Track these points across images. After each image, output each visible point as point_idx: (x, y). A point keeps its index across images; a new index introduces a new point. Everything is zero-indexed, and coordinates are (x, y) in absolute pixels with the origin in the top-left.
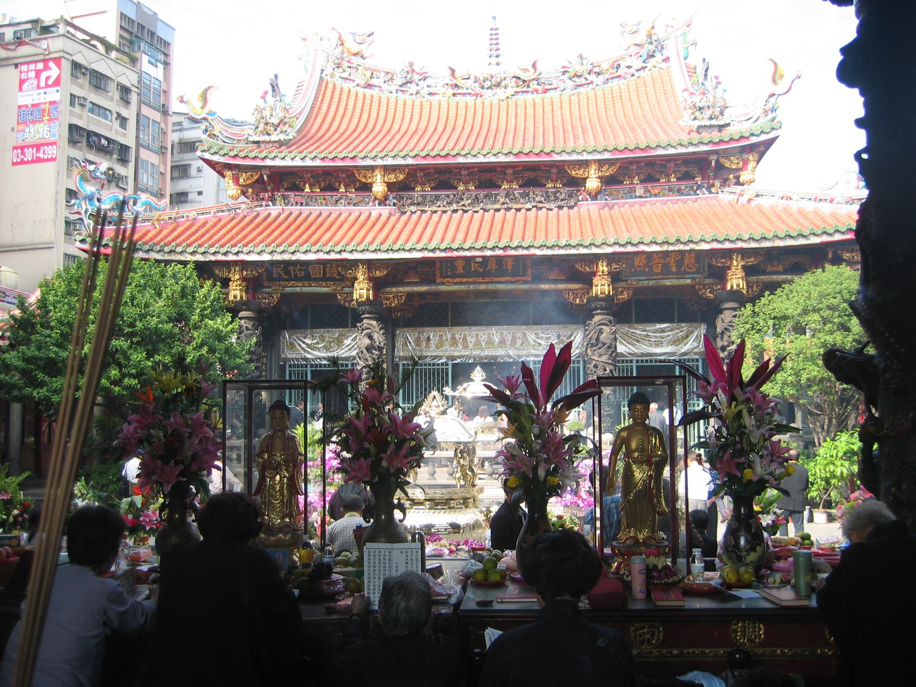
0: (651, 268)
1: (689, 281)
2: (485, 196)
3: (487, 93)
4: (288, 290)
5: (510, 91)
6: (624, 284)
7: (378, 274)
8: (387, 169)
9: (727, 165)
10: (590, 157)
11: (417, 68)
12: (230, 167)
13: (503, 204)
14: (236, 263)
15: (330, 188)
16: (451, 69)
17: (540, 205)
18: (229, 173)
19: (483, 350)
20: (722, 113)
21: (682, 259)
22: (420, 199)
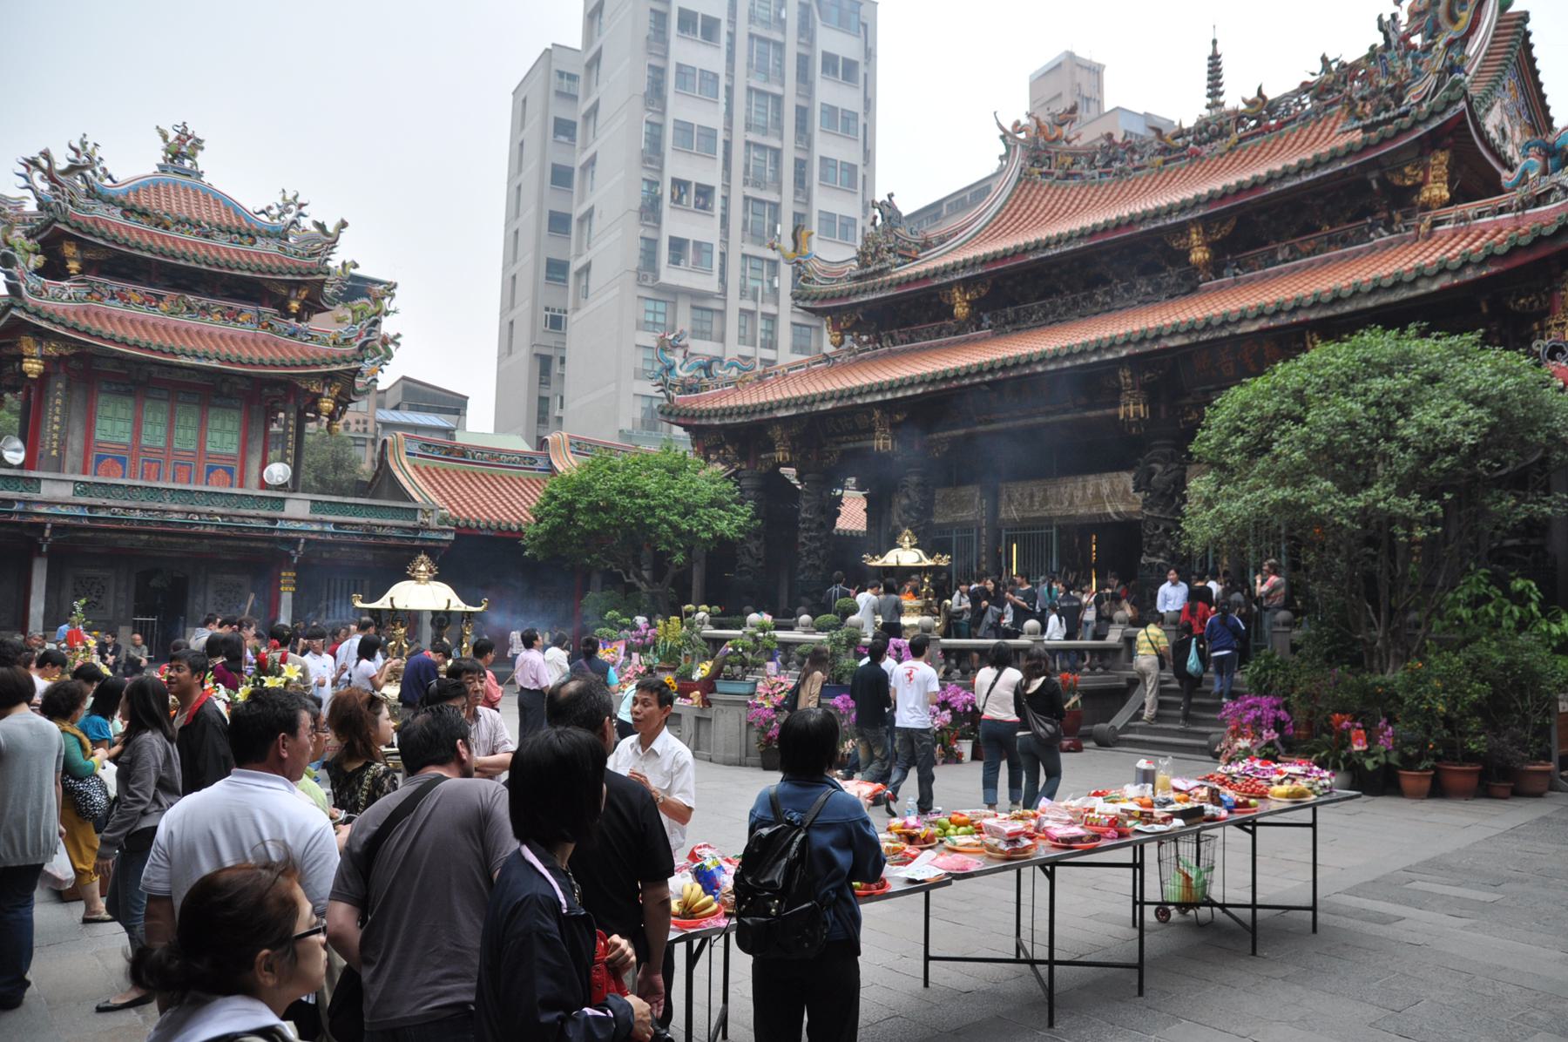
2: (1084, 298)
3: (1206, 149)
4: (844, 446)
5: (1234, 138)
6: (1189, 400)
9: (1397, 181)
10: (1182, 218)
11: (1118, 138)
13: (1104, 304)
14: (777, 420)
16: (1153, 129)
19: (1090, 506)
20: (1399, 101)
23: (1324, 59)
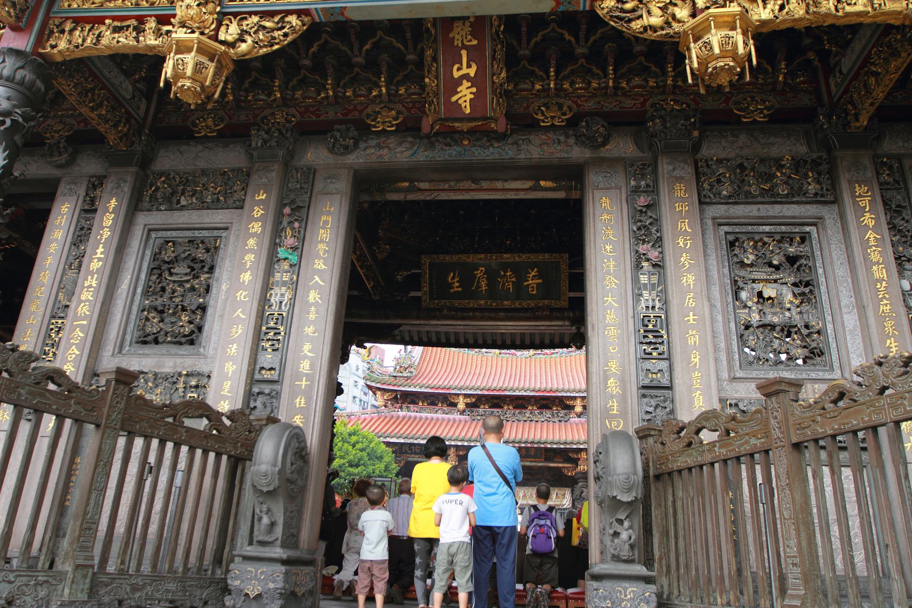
4: (410, 459)
7: (461, 453)
8: (466, 396)
12: (379, 389)
15: (433, 404)
18: (379, 393)
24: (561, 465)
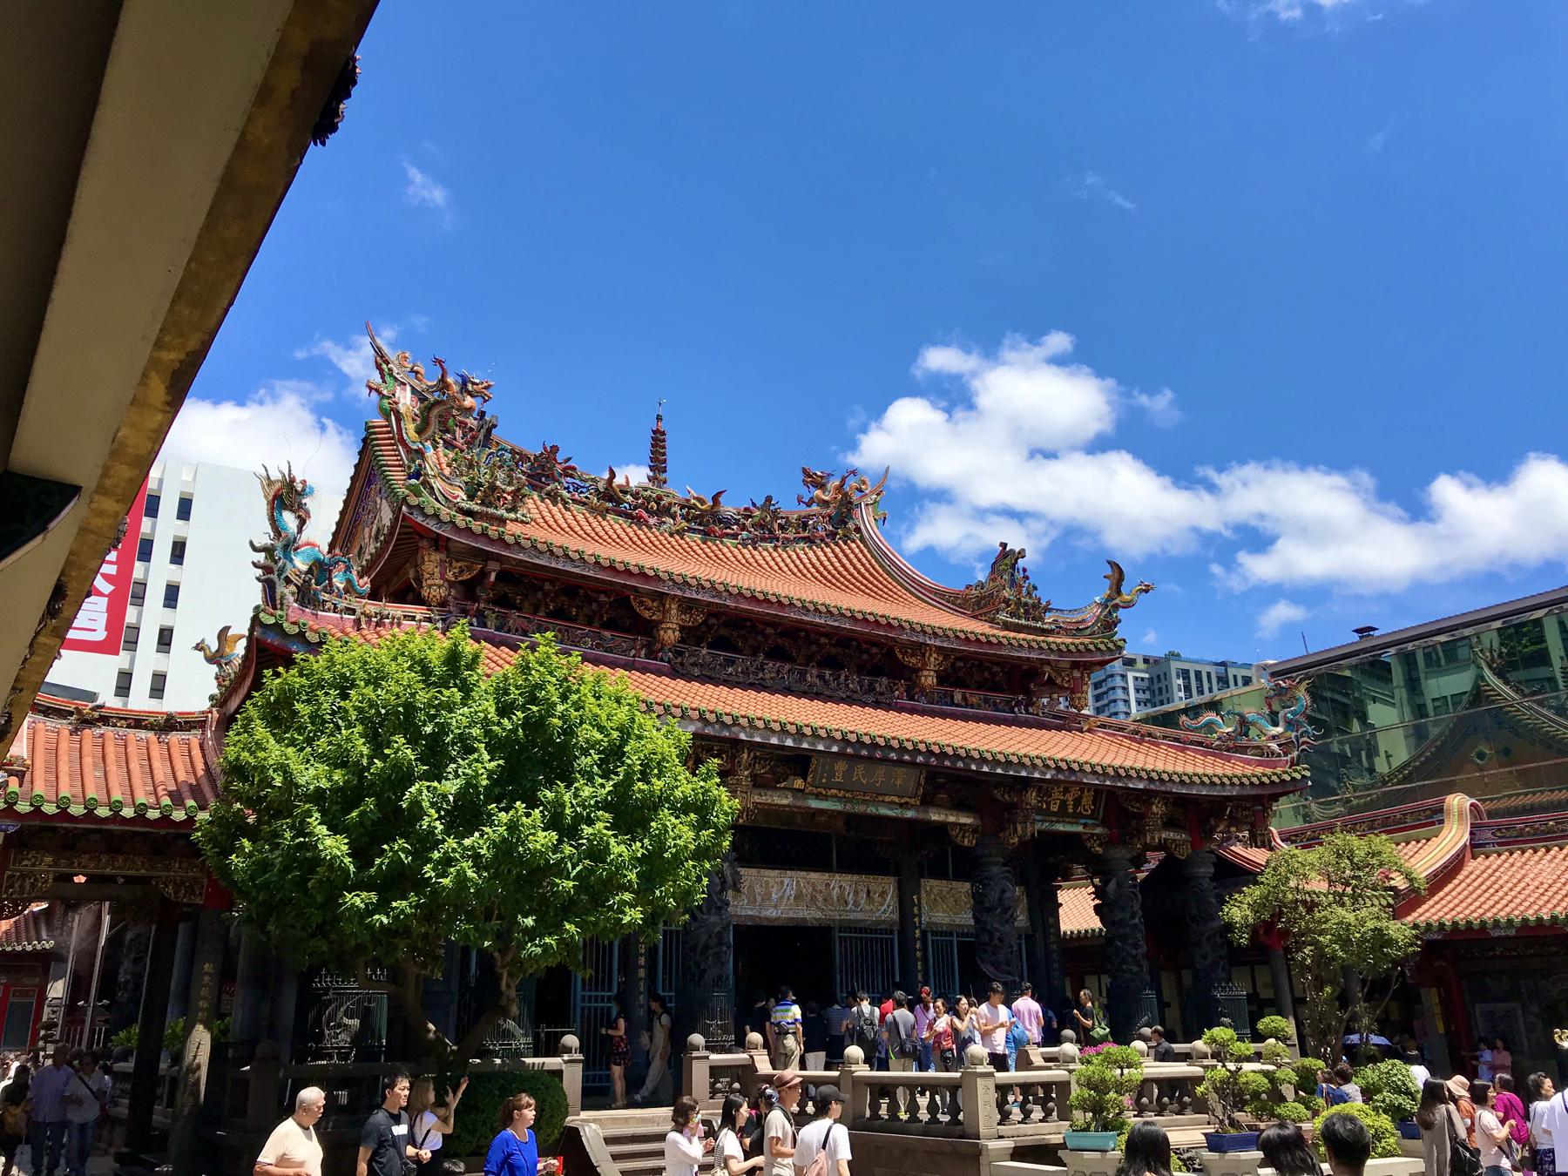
0: (1048, 804)
1: (1080, 829)
3: (652, 521)
9: (1059, 681)
11: (560, 457)
17: (855, 696)
21: (1080, 798)
22: (709, 659)
23: (769, 499)
24: (952, 819)
